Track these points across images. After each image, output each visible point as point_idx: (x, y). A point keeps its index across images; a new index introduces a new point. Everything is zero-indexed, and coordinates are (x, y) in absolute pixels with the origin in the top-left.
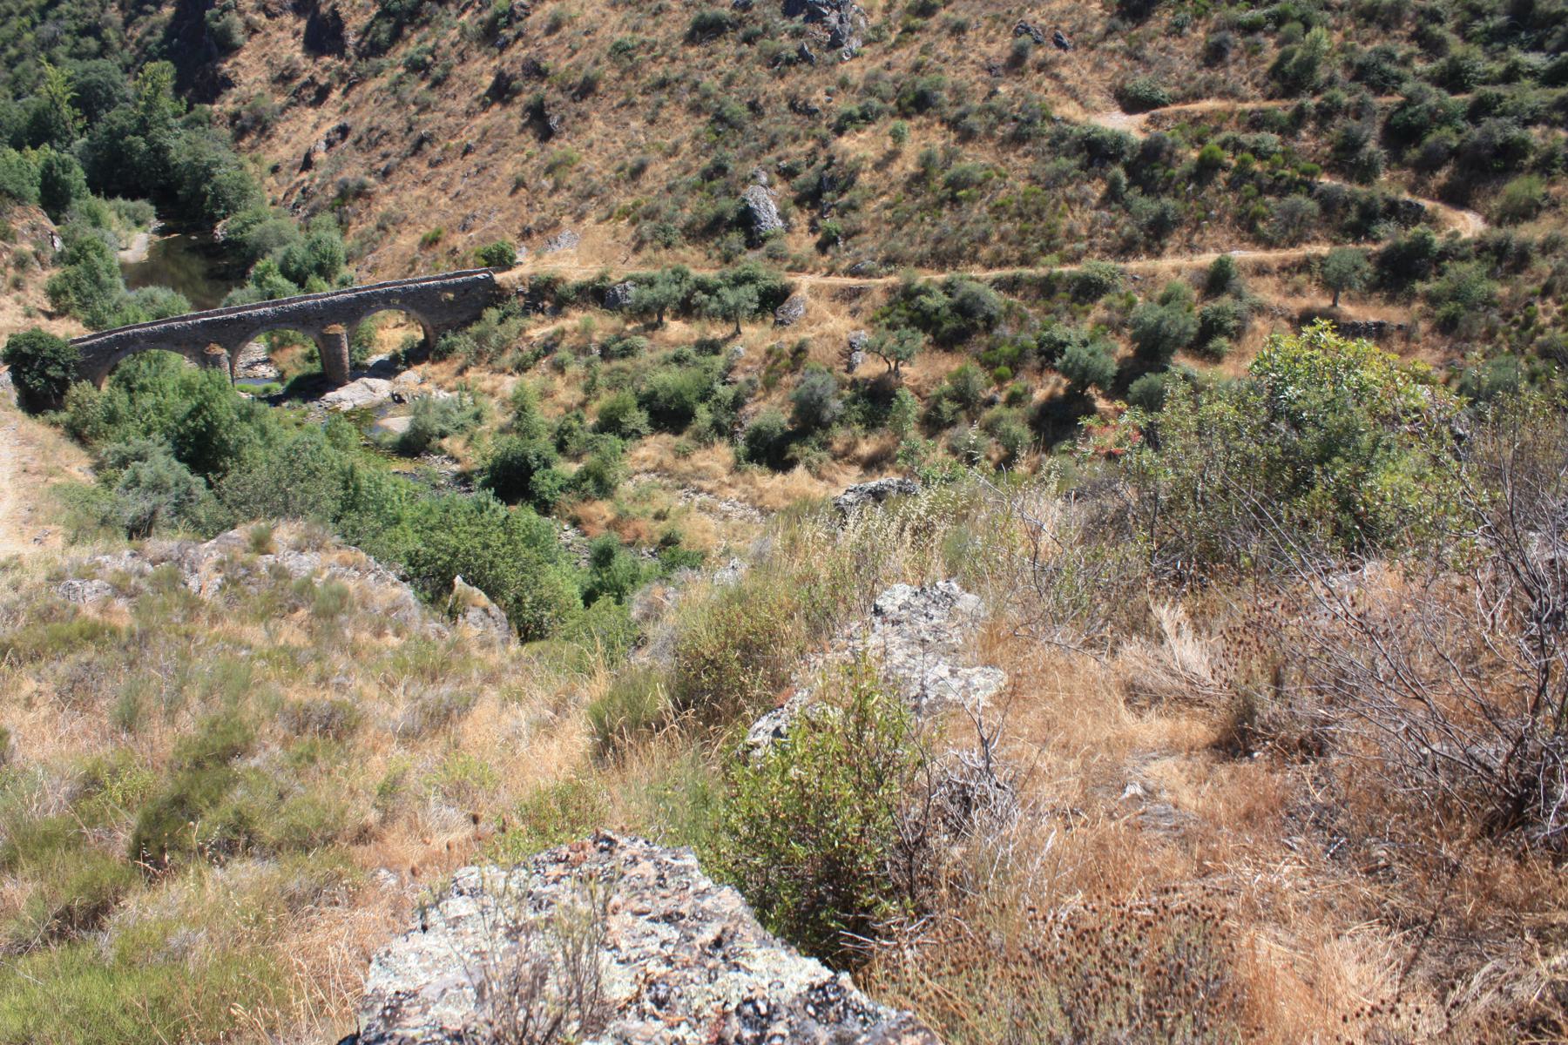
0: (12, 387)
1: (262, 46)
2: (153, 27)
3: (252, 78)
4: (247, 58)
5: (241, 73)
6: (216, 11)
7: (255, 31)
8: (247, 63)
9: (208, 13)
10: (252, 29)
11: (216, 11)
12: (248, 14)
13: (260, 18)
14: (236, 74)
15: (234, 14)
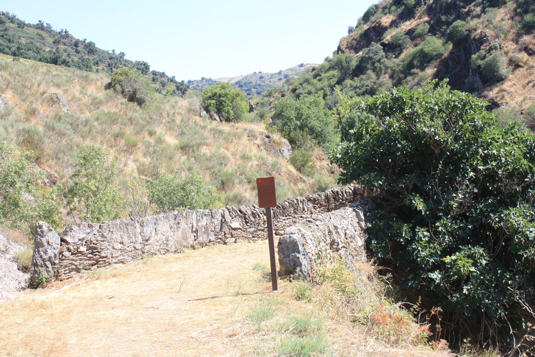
0: (366, 267)
1: (525, 77)
2: (420, 81)
3: (519, 99)
4: (511, 86)
5: (507, 97)
6: (483, 52)
7: (517, 66)
8: (512, 90)
9: (474, 56)
10: (515, 65)
11: (483, 52)
12: (510, 54)
13: (524, 56)
14: (503, 97)
15: (498, 52)
